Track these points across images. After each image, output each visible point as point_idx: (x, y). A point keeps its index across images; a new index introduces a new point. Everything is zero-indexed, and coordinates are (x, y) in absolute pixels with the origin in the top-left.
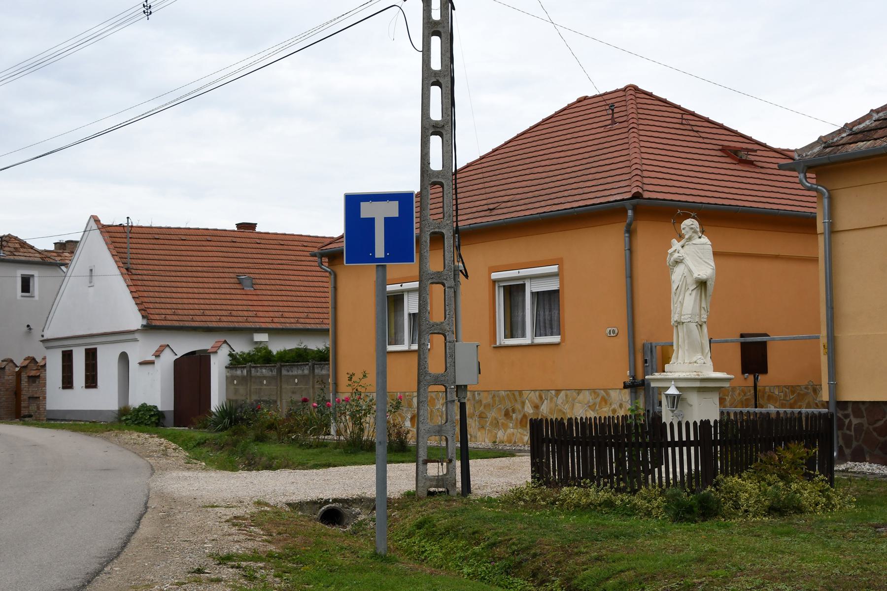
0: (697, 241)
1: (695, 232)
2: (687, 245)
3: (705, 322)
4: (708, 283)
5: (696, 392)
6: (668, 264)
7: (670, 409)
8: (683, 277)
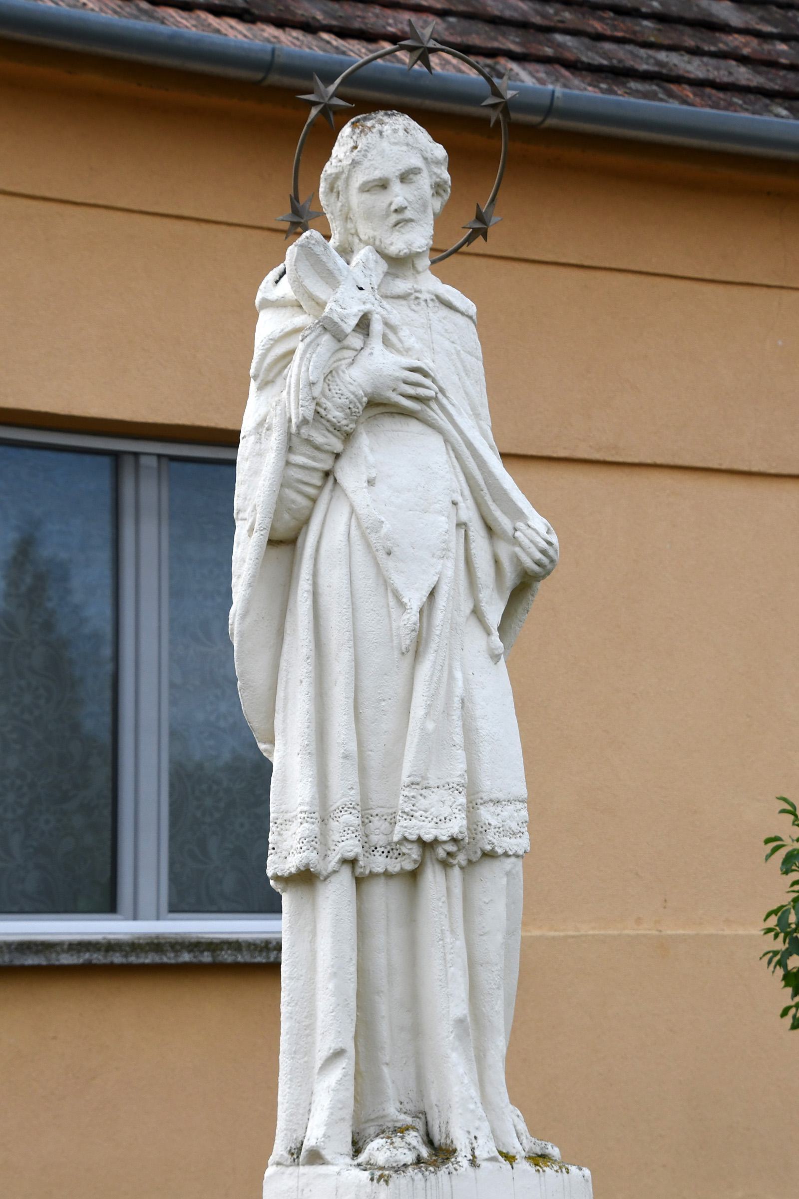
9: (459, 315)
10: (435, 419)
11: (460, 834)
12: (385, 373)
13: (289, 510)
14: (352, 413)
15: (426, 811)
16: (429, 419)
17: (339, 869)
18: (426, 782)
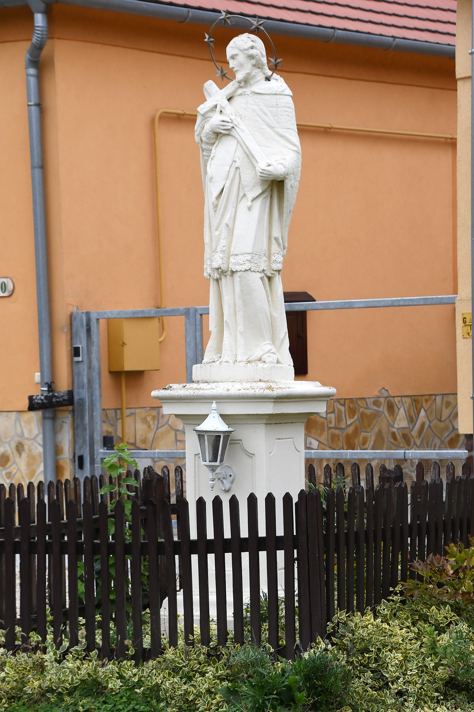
0: (261, 86)
1: (258, 66)
2: (241, 95)
3: (279, 271)
4: (288, 184)
5: (263, 426)
6: (197, 139)
7: (207, 463)
8: (233, 170)
9: (265, 95)
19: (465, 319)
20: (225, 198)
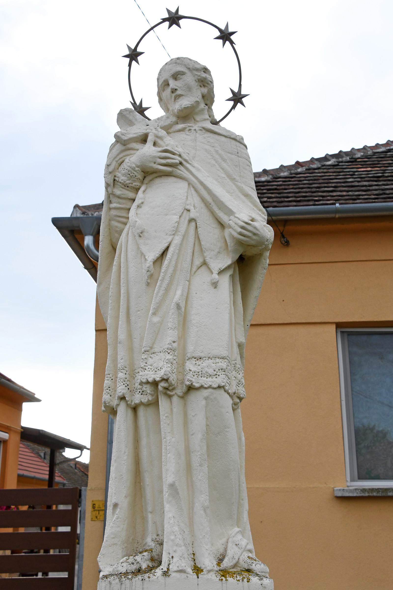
9: (222, 137)
10: (181, 174)
11: (165, 376)
12: (146, 155)
13: (116, 231)
14: (131, 176)
15: (151, 365)
16: (179, 174)
17: (120, 403)
18: (154, 350)
19: (94, 506)
20: (173, 263)
